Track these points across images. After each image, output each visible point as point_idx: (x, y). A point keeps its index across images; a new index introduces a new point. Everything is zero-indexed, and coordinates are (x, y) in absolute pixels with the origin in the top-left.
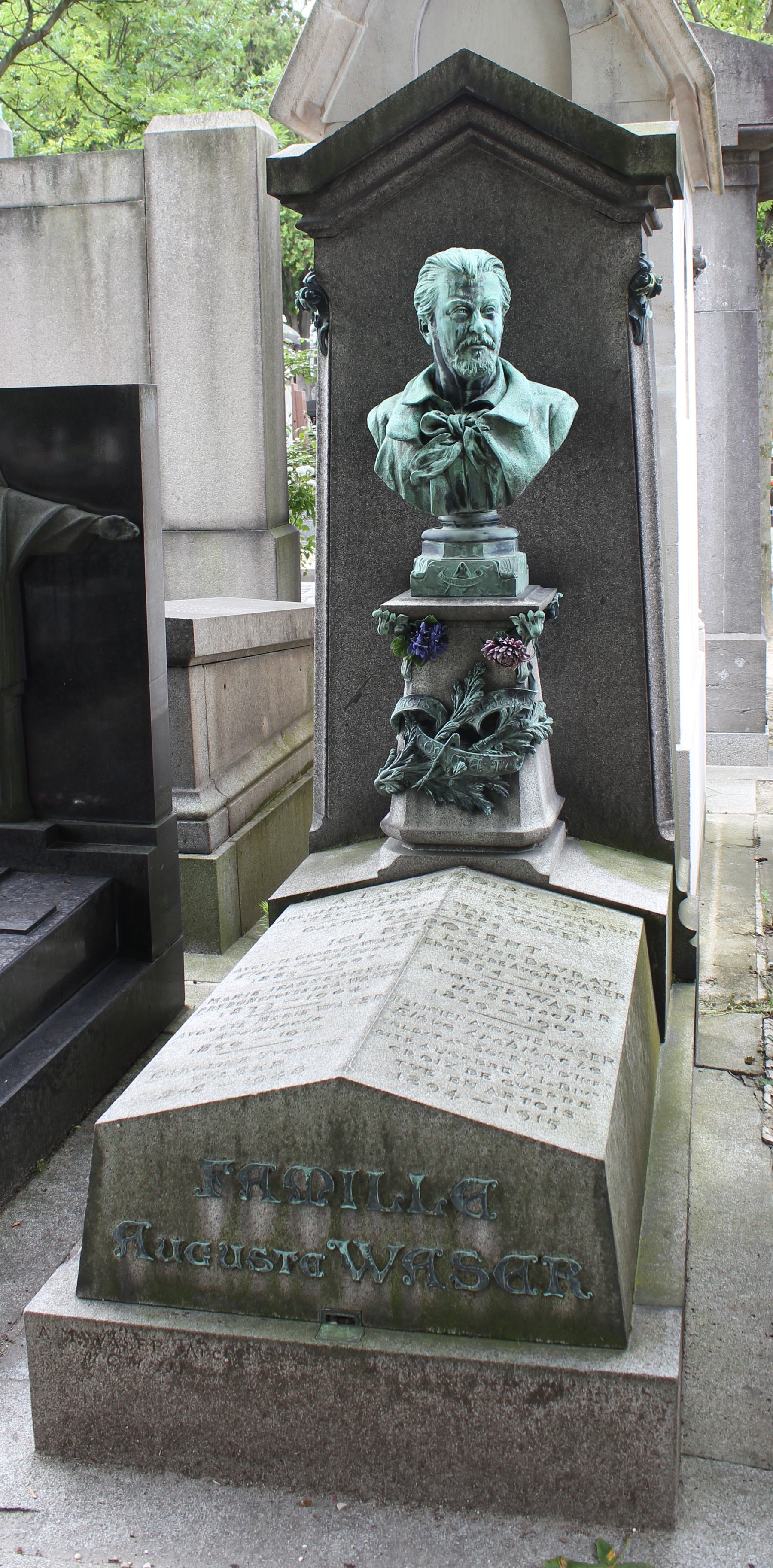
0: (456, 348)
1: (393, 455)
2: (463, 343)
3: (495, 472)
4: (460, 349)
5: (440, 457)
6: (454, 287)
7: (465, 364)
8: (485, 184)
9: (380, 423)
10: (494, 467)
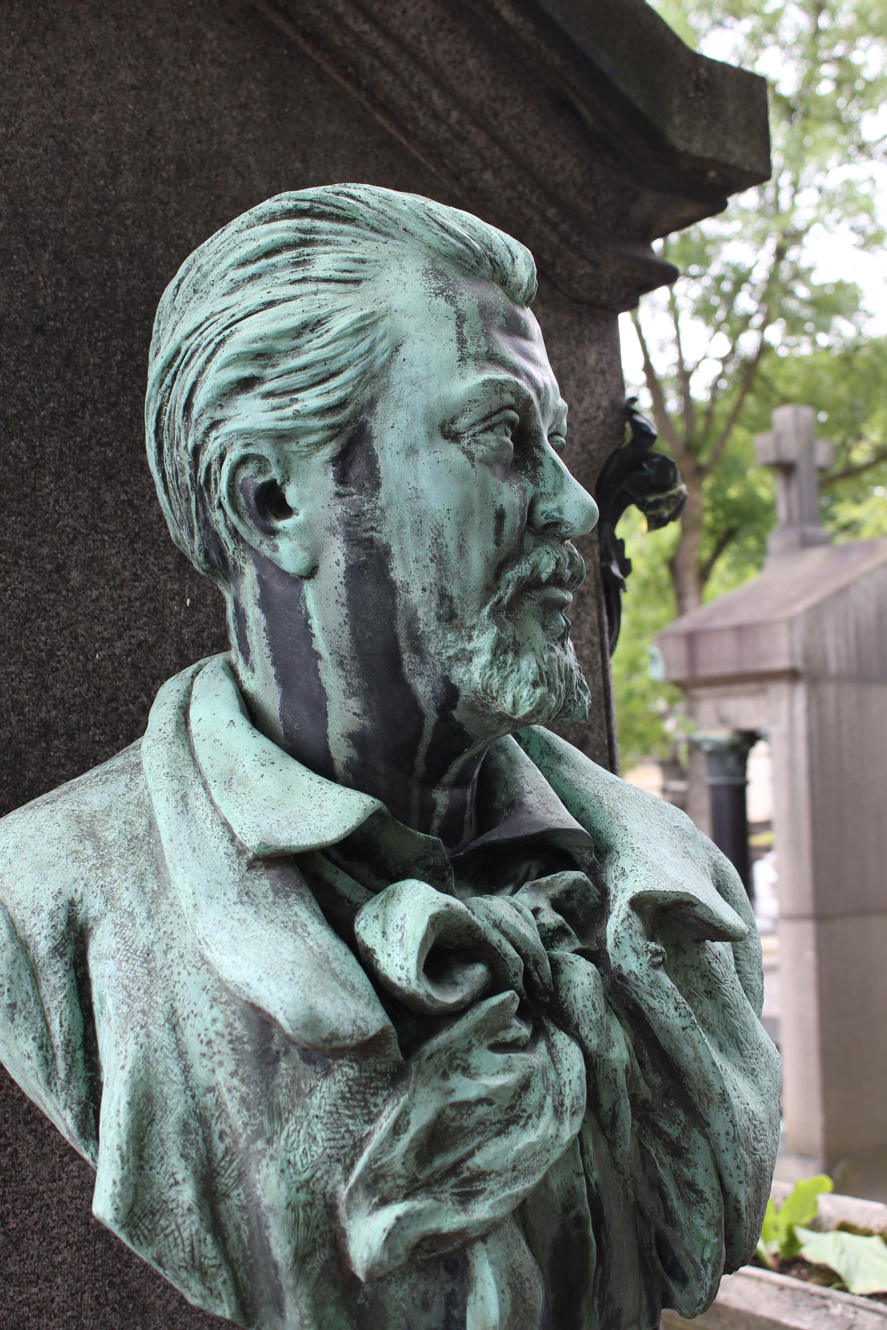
0: (490, 589)
1: (200, 1123)
2: (522, 569)
3: (677, 1151)
4: (507, 592)
5: (511, 1112)
6: (473, 323)
7: (528, 666)
8: (213, 71)
9: (43, 946)
10: (674, 1132)
